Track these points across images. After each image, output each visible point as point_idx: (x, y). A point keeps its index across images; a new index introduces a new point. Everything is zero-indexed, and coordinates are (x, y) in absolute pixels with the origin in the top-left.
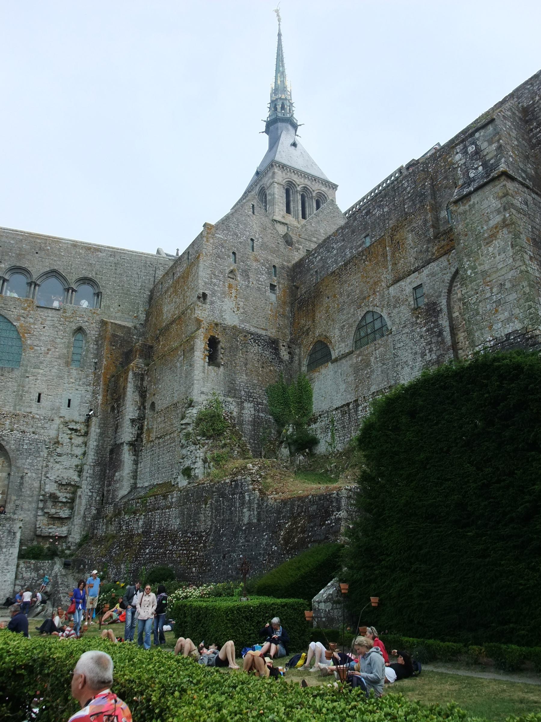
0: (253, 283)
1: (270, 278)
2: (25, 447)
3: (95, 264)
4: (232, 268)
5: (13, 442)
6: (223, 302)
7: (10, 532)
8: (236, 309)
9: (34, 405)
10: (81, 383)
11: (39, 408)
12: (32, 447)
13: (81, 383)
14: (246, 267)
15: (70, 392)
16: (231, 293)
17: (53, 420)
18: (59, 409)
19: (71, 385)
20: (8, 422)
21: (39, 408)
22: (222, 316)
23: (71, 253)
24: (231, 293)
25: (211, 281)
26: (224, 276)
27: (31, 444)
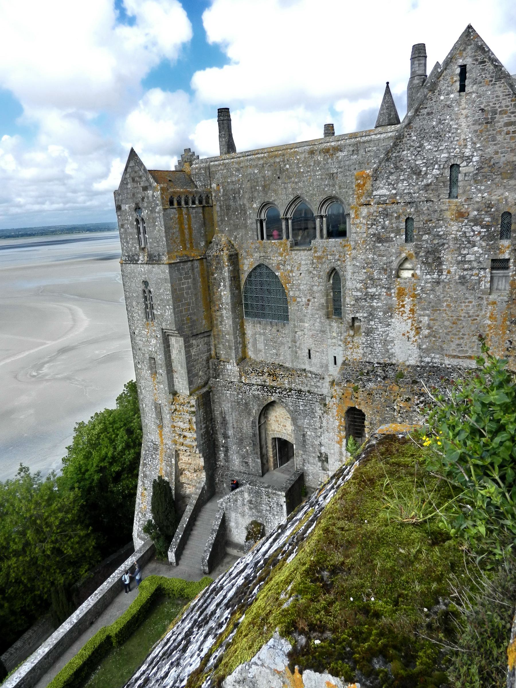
0: (449, 272)
1: (487, 251)
2: (301, 408)
3: (337, 173)
4: (404, 255)
5: (290, 404)
6: (388, 325)
7: (278, 504)
8: (413, 333)
9: (307, 362)
10: (342, 337)
11: (311, 366)
12: (307, 408)
13: (342, 337)
14: (436, 242)
15: (334, 348)
16: (403, 306)
17: (323, 378)
18: (327, 366)
19: (334, 341)
20: (286, 382)
21: (311, 366)
22: (387, 351)
23: (310, 166)
24: (403, 306)
25: (367, 294)
26: (389, 277)
27: (306, 406)
